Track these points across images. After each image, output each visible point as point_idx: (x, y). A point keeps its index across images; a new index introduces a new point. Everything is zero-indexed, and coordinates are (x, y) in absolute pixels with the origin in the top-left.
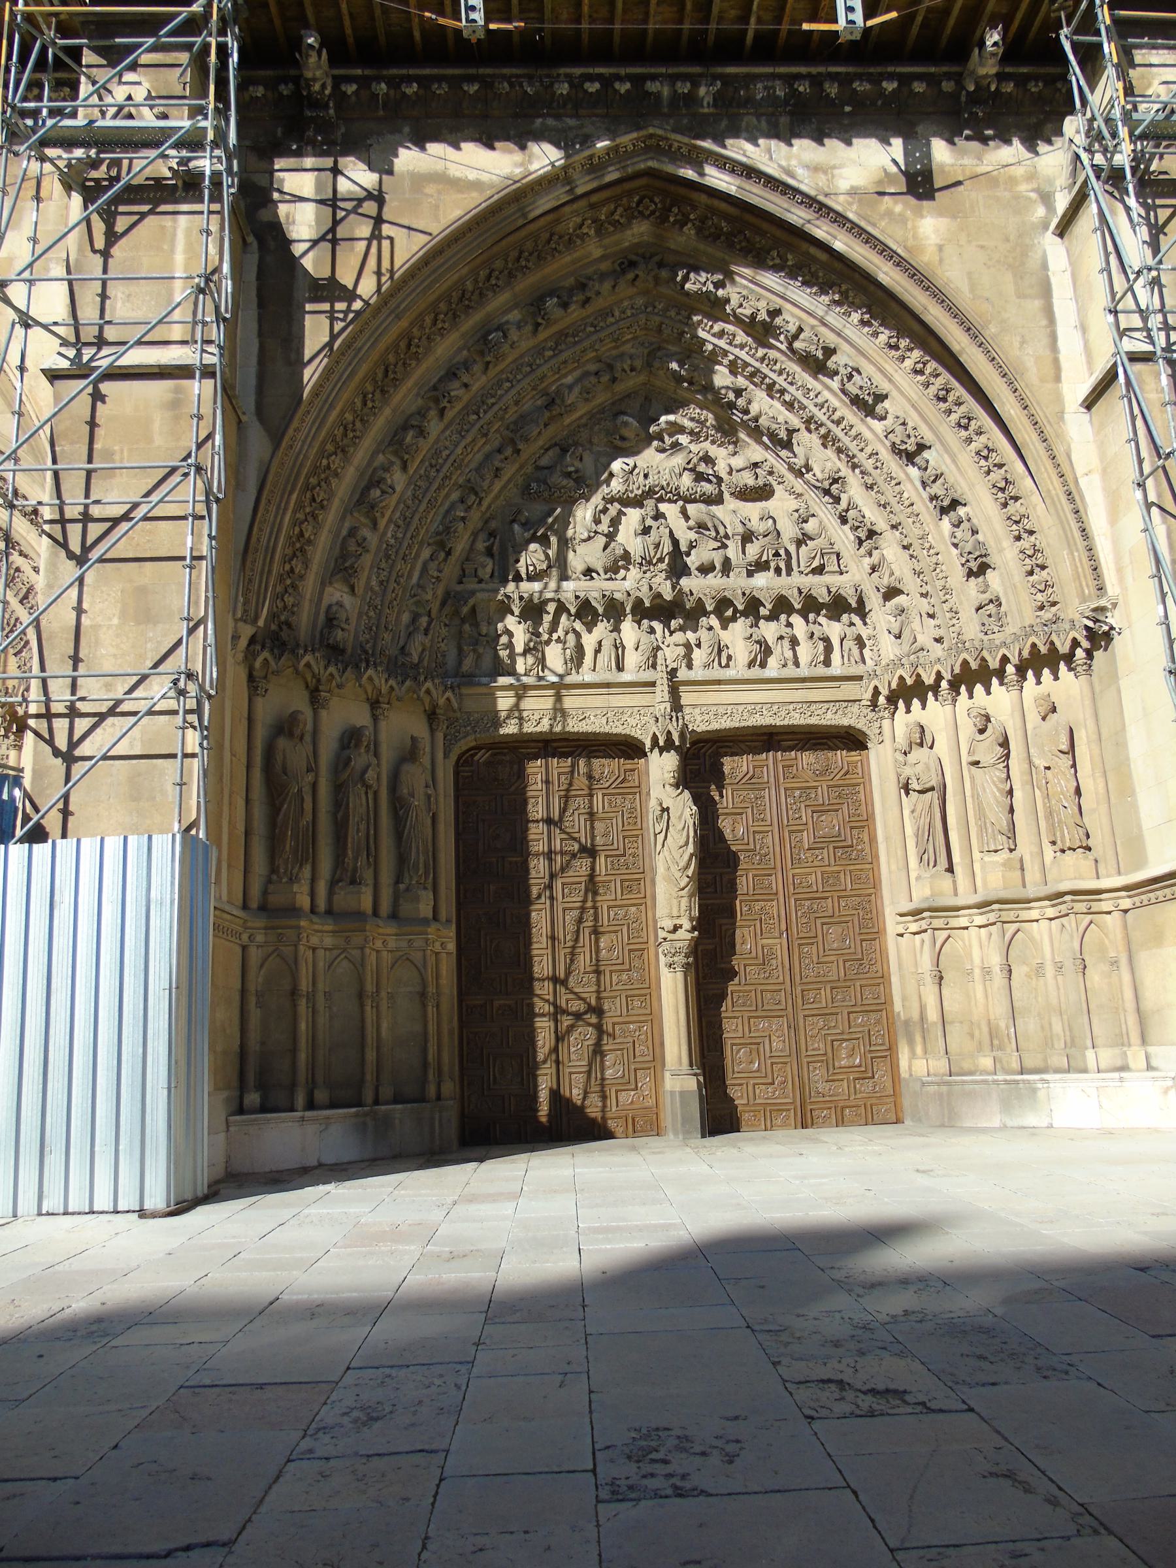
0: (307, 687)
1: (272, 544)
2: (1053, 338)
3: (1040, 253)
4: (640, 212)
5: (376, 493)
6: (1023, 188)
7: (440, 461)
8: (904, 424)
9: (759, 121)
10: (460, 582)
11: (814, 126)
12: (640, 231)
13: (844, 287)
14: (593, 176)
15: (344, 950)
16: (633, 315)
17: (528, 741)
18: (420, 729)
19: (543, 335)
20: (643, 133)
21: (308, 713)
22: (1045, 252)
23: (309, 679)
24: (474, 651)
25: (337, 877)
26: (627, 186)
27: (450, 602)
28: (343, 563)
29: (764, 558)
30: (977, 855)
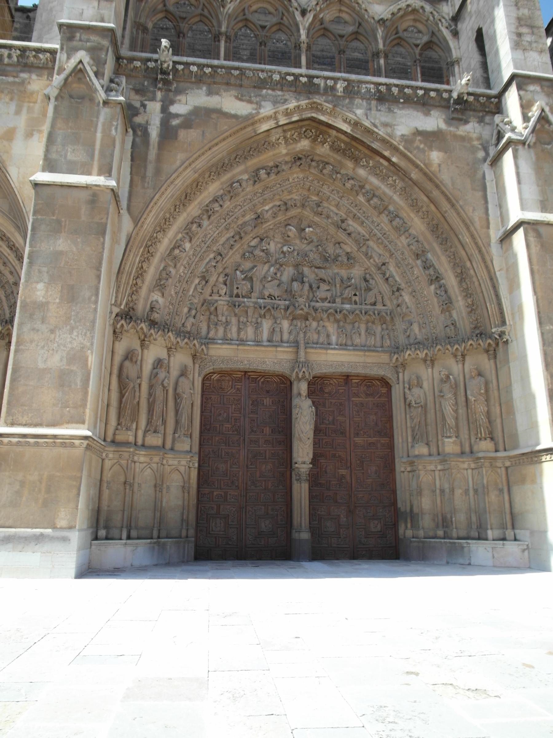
1: (130, 270)
2: (487, 209)
3: (482, 172)
5: (177, 252)
6: (476, 143)
7: (207, 239)
10: (211, 296)
12: (304, 144)
13: (394, 178)
14: (287, 117)
15: (149, 464)
16: (298, 181)
17: (237, 371)
18: (189, 361)
19: (257, 186)
20: (310, 101)
21: (140, 351)
23: (141, 335)
24: (215, 327)
25: (148, 429)
26: (301, 124)
27: (205, 304)
28: (160, 282)
29: (350, 296)
30: (440, 437)
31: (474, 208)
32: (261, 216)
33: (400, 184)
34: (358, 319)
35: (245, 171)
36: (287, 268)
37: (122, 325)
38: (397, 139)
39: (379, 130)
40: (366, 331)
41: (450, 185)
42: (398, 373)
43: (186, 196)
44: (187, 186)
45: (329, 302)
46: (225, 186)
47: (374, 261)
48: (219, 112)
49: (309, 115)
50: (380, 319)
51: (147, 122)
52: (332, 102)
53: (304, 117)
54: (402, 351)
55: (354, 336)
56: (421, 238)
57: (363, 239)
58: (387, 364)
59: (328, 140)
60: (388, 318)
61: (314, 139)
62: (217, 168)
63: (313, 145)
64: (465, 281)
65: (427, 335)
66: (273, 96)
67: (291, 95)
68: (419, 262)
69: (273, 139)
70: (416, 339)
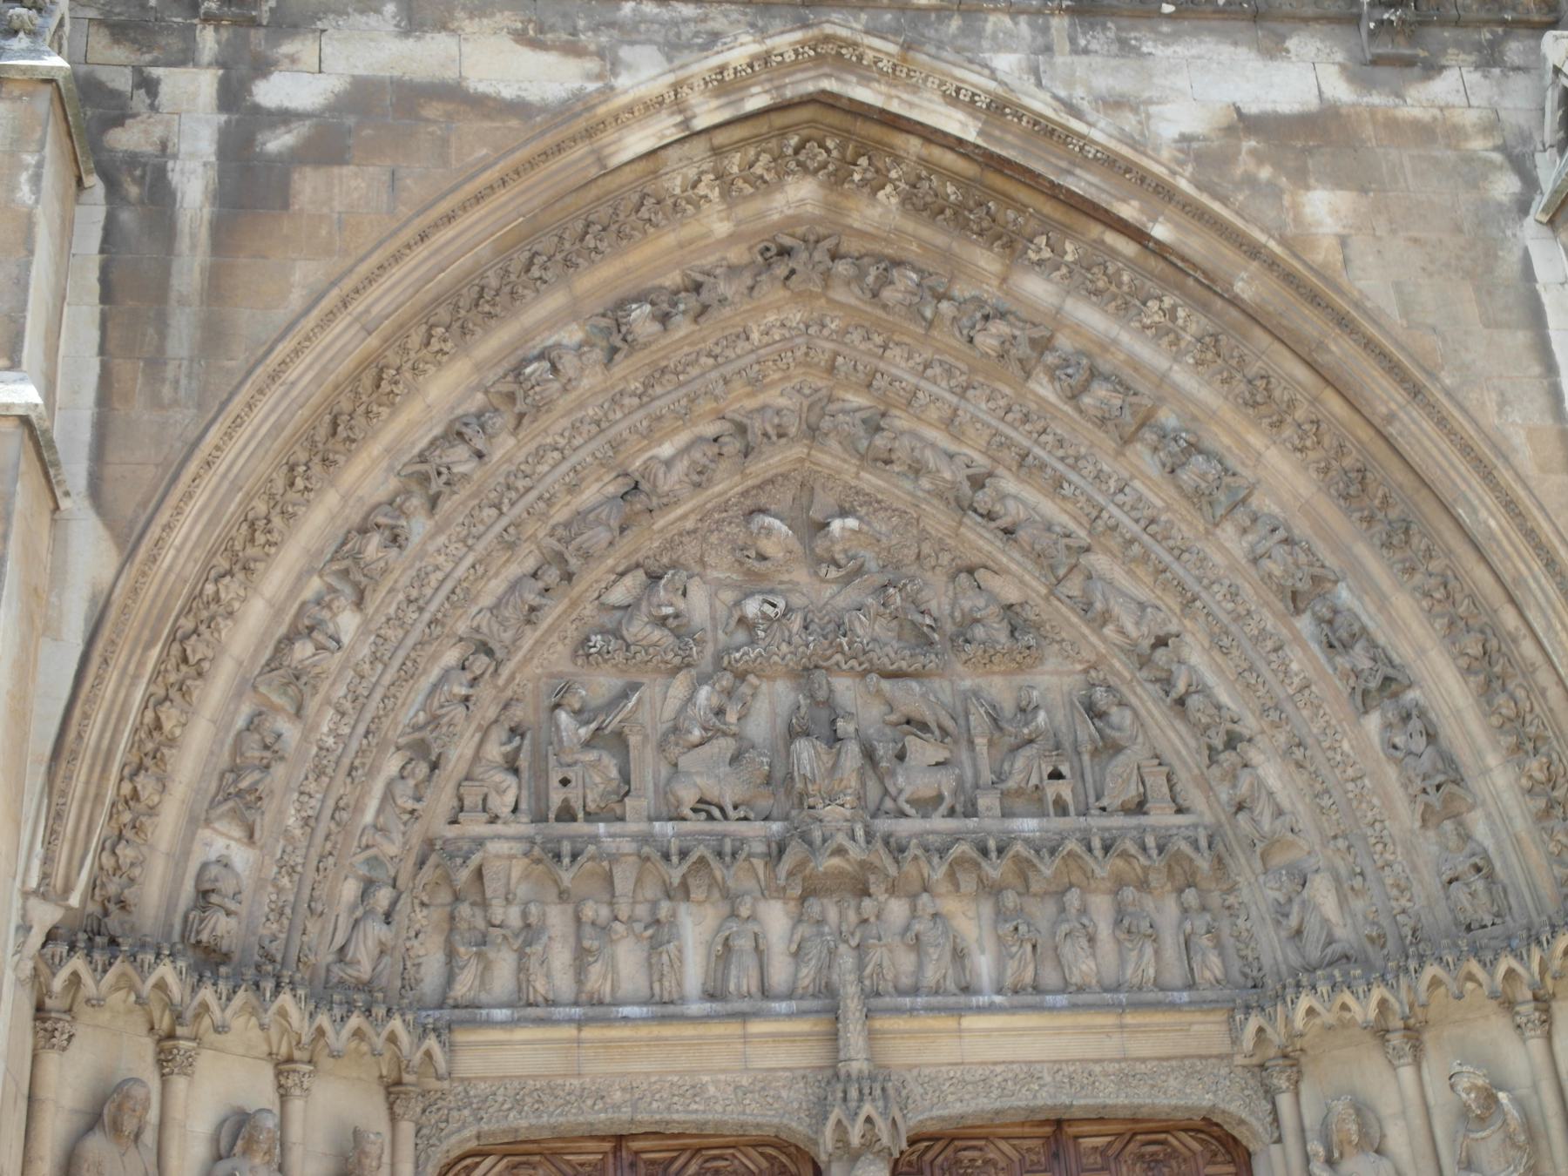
0: (152, 1028)
1: (105, 743)
4: (799, 164)
5: (303, 650)
6: (1478, 145)
7: (428, 591)
8: (1286, 541)
9: (1016, 24)
10: (454, 822)
11: (1111, 34)
13: (1168, 302)
14: (723, 100)
16: (784, 339)
17: (583, 1138)
18: (369, 1111)
19: (621, 367)
20: (811, 33)
21: (154, 1083)
22: (1526, 251)
23: (156, 1014)
24: (479, 955)
26: (779, 120)
27: (433, 859)
28: (235, 782)
29: (1034, 780)
31: (1502, 394)
32: (644, 486)
33: (1192, 324)
34: (1076, 876)
35: (572, 313)
36: (764, 687)
37: (75, 979)
38: (1165, 155)
39: (1090, 125)
40: (1118, 922)
41: (1393, 311)
42: (1270, 1094)
43: (335, 425)
44: (336, 387)
45: (952, 813)
46: (491, 377)
47: (1121, 631)
48: (454, 95)
49: (810, 87)
50: (1170, 867)
51: (164, 145)
52: (897, 32)
53: (789, 93)
54: (1279, 997)
55: (1067, 950)
56: (1301, 529)
57: (1068, 547)
58: (1220, 1057)
59: (893, 174)
60: (1203, 863)
61: (834, 173)
62: (457, 307)
63: (833, 198)
64: (1504, 686)
65: (1374, 923)
66: (663, 24)
67: (735, 16)
68: (1305, 624)
69: (675, 184)
70: (1330, 941)
